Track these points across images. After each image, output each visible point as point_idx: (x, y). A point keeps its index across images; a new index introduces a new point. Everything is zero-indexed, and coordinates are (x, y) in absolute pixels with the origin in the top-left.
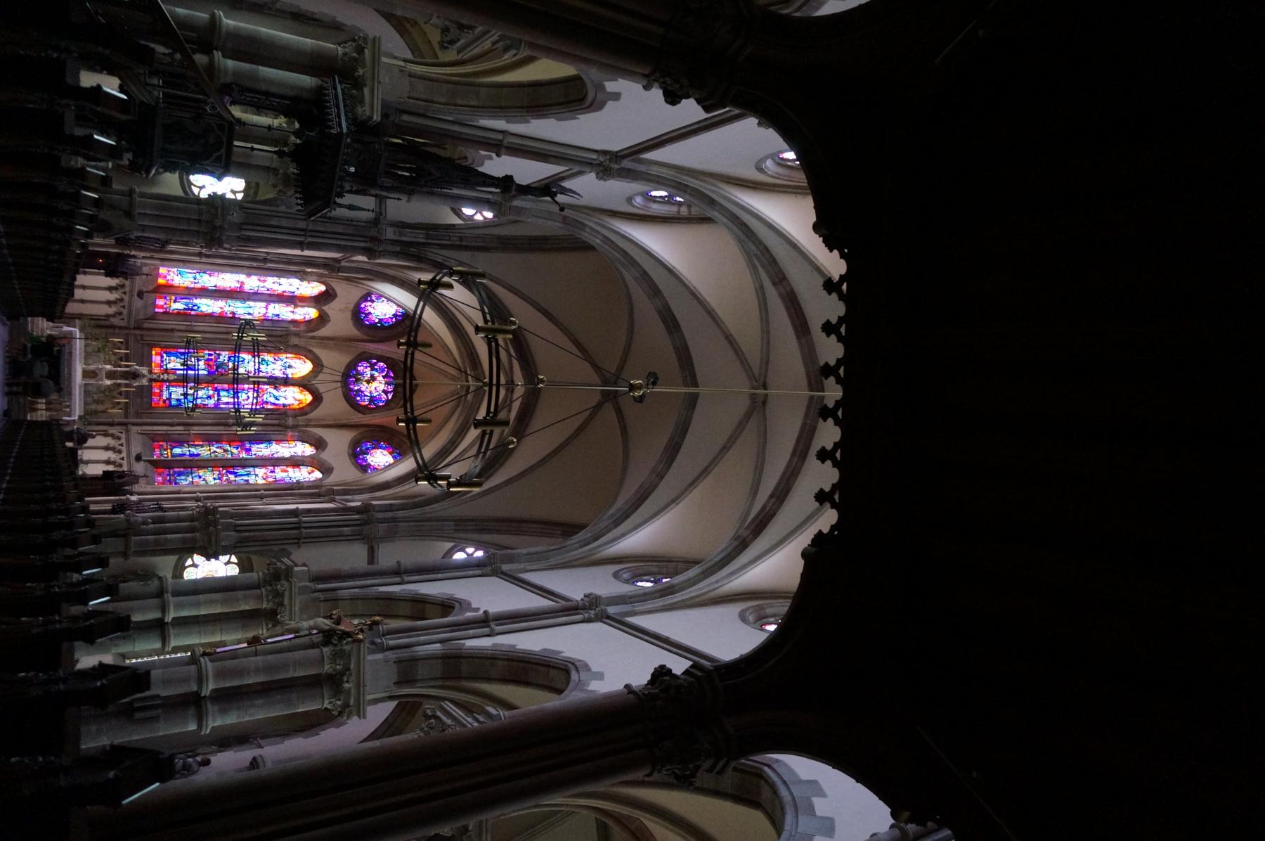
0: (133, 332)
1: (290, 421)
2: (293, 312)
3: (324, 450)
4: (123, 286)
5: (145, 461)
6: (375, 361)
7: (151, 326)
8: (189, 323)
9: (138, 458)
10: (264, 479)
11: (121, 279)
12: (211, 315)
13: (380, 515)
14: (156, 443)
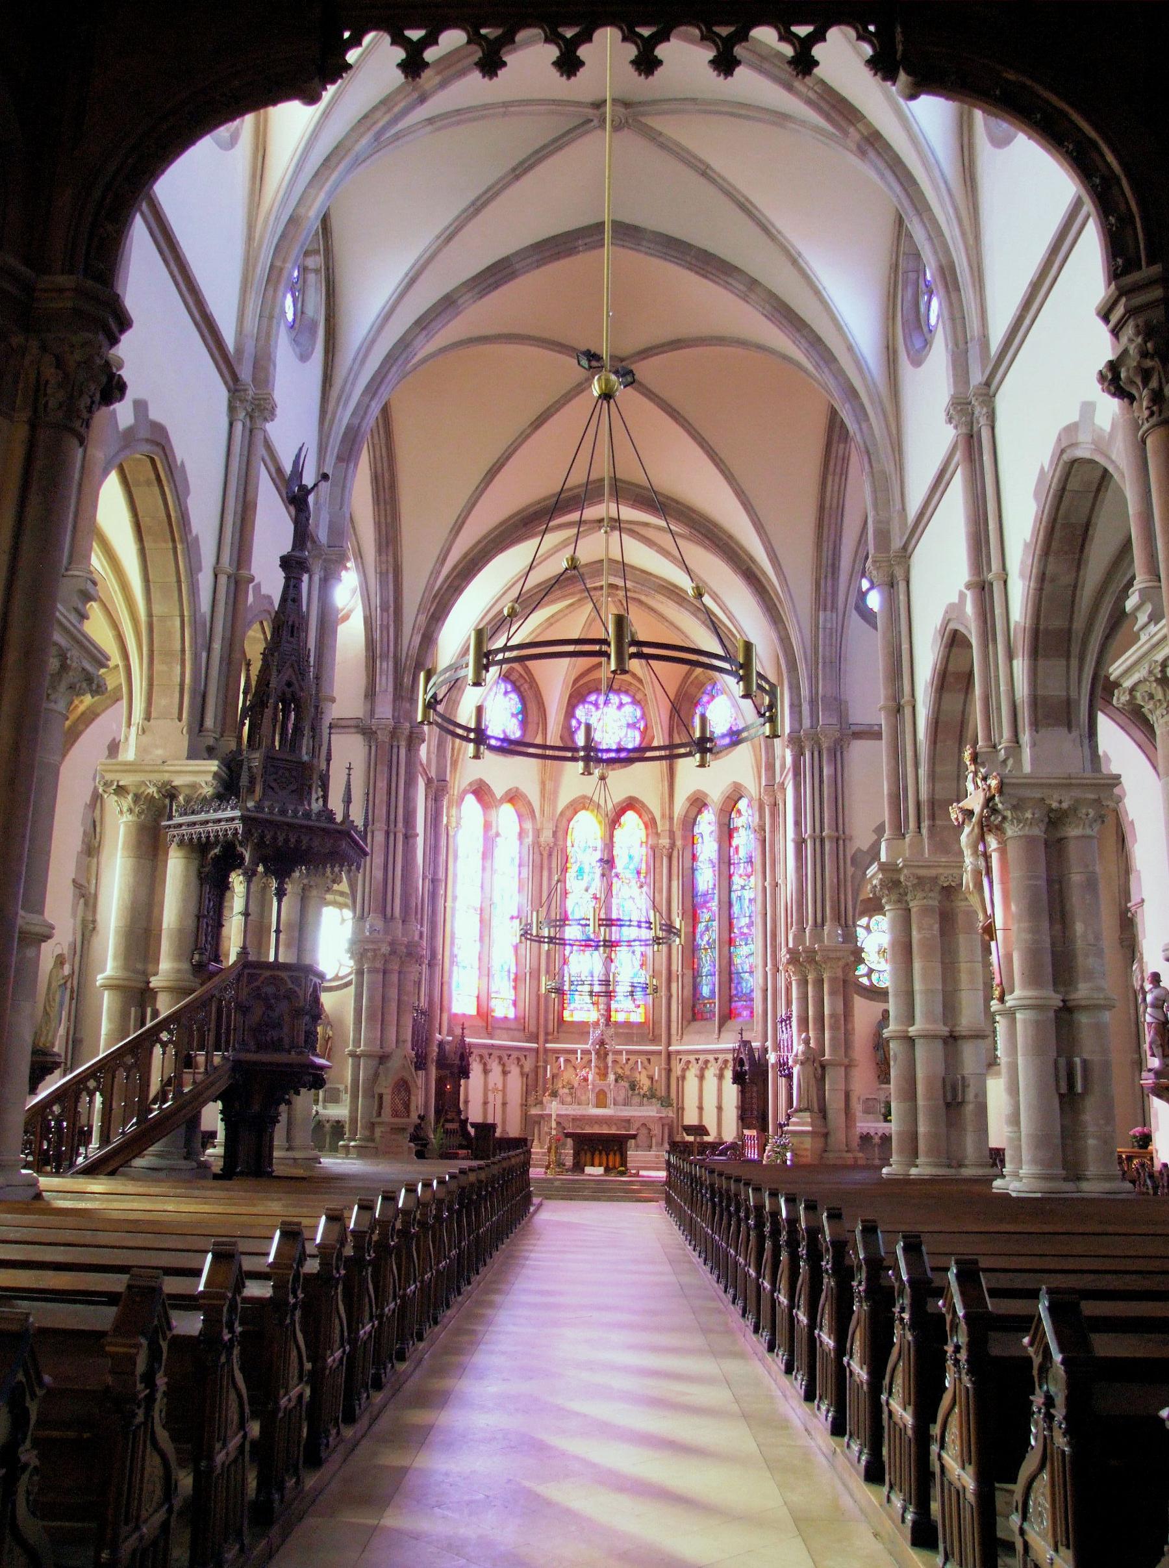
3: (706, 795)
4: (481, 1057)
11: (471, 1059)
13: (807, 723)
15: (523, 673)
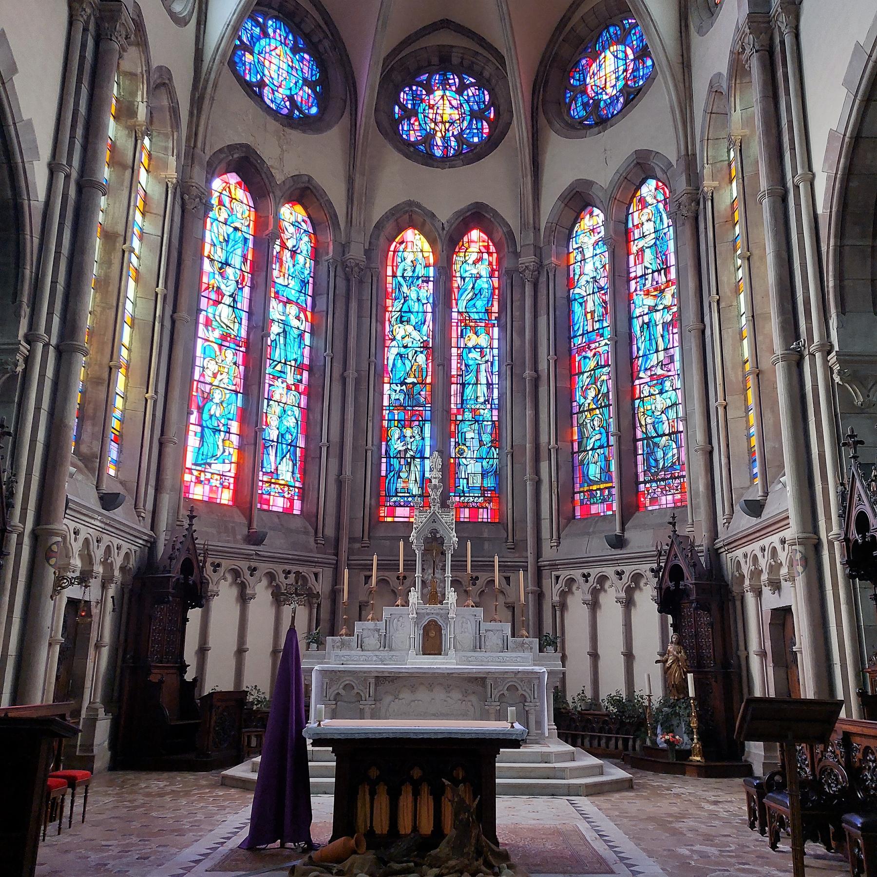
0: (344, 556)
1: (528, 259)
2: (294, 253)
5: (623, 530)
6: (397, 108)
7: (331, 522)
8: (324, 450)
9: (618, 542)
10: (662, 291)
12: (306, 412)
14: (578, 513)
15: (322, 23)
